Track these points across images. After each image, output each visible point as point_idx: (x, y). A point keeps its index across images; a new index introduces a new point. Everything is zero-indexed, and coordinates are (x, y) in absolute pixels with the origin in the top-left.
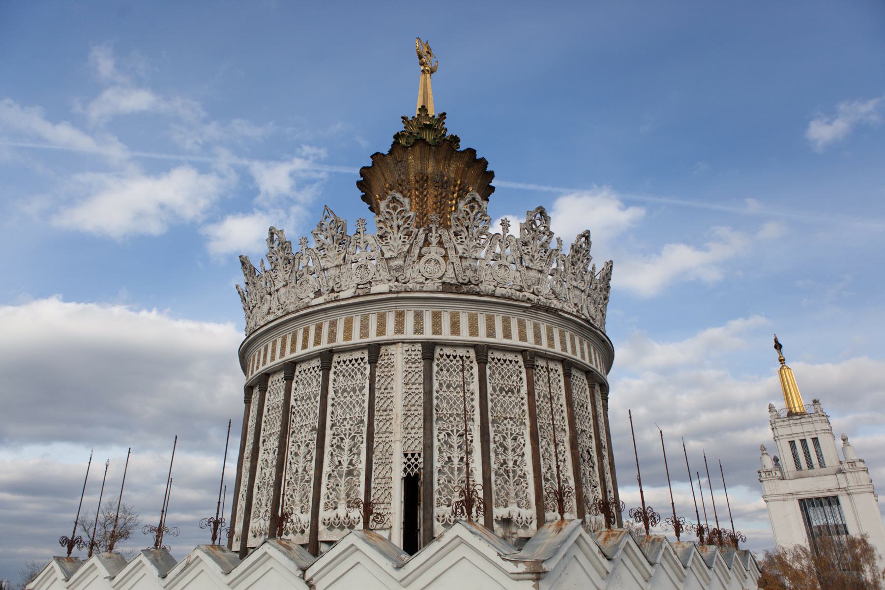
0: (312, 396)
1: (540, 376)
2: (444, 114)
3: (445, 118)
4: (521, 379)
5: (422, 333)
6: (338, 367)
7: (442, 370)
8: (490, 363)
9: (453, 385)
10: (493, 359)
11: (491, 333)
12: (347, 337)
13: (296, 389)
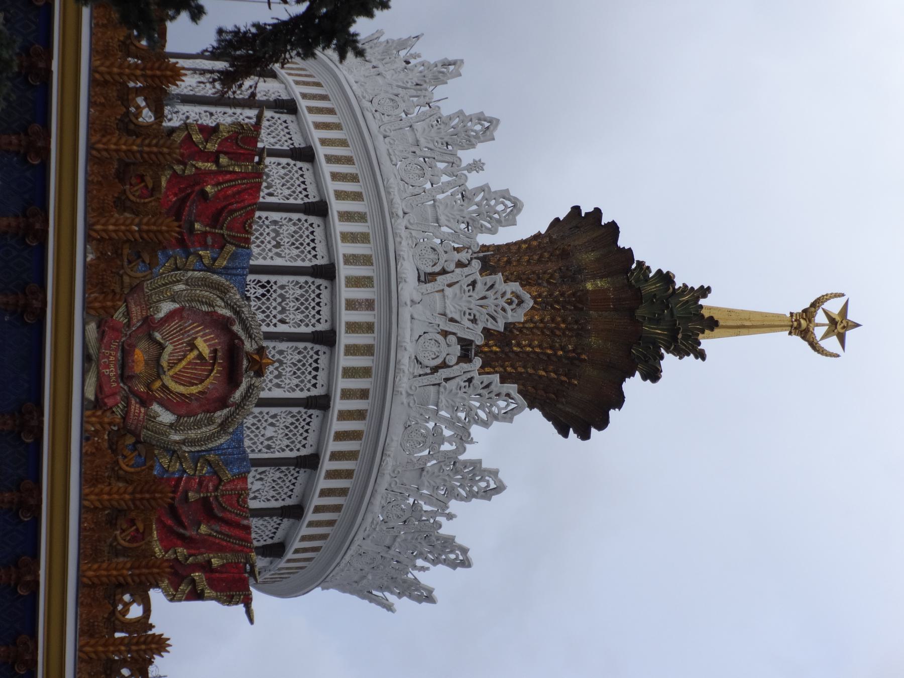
0: (271, 190)
1: (286, 475)
2: (703, 358)
3: (697, 357)
4: (283, 450)
5: (346, 332)
6: (306, 225)
7: (299, 353)
8: (306, 413)
9: (282, 368)
10: (310, 416)
11: (344, 415)
12: (346, 237)
13: (279, 164)
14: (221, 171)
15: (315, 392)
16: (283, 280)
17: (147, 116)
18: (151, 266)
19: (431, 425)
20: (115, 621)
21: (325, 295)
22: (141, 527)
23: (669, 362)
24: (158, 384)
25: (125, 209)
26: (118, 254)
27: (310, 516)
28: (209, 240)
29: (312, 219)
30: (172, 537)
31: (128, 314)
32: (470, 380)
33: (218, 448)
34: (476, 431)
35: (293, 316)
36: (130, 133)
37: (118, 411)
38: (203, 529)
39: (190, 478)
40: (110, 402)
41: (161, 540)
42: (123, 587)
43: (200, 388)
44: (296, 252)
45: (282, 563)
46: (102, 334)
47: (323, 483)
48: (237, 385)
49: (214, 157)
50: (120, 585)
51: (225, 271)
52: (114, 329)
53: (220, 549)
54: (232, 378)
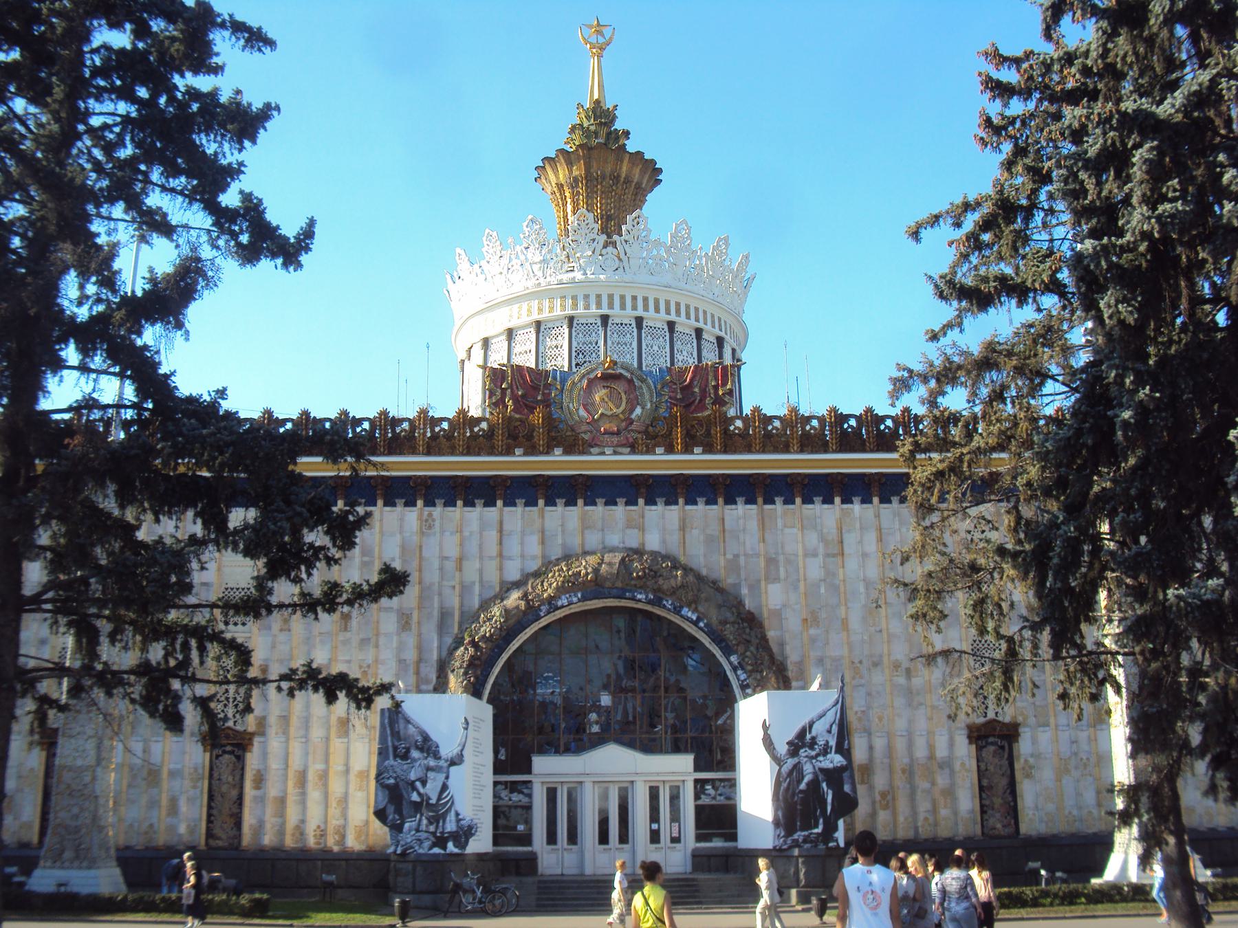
14: (511, 386)
15: (634, 325)
16: (574, 344)
17: (484, 425)
18: (561, 422)
19: (650, 261)
20: (744, 435)
21: (584, 321)
22: (695, 422)
23: (619, 125)
24: (621, 416)
25: (532, 436)
26: (554, 439)
27: (701, 325)
28: (547, 391)
29: (542, 329)
30: (702, 407)
31: (585, 432)
32: (626, 241)
33: (654, 383)
34: (653, 237)
35: (593, 338)
36: (493, 434)
37: (635, 435)
38: (696, 390)
39: (670, 398)
40: (631, 440)
41: (702, 411)
42: (726, 432)
43: (623, 394)
44: (560, 337)
45: (727, 338)
46: (596, 445)
47: (683, 318)
48: (621, 374)
49: (504, 391)
50: (725, 433)
51: (563, 381)
52: (593, 439)
53: (707, 379)
54: (619, 377)
